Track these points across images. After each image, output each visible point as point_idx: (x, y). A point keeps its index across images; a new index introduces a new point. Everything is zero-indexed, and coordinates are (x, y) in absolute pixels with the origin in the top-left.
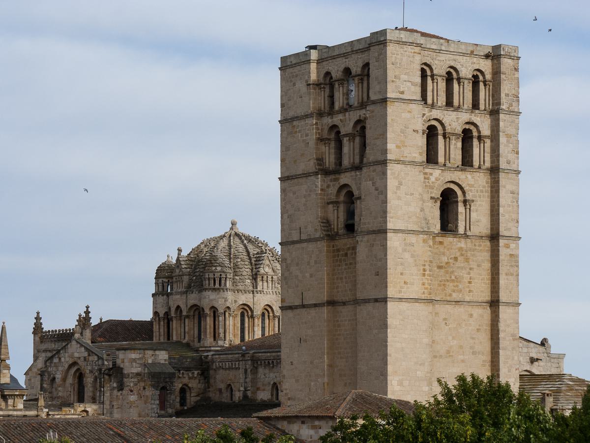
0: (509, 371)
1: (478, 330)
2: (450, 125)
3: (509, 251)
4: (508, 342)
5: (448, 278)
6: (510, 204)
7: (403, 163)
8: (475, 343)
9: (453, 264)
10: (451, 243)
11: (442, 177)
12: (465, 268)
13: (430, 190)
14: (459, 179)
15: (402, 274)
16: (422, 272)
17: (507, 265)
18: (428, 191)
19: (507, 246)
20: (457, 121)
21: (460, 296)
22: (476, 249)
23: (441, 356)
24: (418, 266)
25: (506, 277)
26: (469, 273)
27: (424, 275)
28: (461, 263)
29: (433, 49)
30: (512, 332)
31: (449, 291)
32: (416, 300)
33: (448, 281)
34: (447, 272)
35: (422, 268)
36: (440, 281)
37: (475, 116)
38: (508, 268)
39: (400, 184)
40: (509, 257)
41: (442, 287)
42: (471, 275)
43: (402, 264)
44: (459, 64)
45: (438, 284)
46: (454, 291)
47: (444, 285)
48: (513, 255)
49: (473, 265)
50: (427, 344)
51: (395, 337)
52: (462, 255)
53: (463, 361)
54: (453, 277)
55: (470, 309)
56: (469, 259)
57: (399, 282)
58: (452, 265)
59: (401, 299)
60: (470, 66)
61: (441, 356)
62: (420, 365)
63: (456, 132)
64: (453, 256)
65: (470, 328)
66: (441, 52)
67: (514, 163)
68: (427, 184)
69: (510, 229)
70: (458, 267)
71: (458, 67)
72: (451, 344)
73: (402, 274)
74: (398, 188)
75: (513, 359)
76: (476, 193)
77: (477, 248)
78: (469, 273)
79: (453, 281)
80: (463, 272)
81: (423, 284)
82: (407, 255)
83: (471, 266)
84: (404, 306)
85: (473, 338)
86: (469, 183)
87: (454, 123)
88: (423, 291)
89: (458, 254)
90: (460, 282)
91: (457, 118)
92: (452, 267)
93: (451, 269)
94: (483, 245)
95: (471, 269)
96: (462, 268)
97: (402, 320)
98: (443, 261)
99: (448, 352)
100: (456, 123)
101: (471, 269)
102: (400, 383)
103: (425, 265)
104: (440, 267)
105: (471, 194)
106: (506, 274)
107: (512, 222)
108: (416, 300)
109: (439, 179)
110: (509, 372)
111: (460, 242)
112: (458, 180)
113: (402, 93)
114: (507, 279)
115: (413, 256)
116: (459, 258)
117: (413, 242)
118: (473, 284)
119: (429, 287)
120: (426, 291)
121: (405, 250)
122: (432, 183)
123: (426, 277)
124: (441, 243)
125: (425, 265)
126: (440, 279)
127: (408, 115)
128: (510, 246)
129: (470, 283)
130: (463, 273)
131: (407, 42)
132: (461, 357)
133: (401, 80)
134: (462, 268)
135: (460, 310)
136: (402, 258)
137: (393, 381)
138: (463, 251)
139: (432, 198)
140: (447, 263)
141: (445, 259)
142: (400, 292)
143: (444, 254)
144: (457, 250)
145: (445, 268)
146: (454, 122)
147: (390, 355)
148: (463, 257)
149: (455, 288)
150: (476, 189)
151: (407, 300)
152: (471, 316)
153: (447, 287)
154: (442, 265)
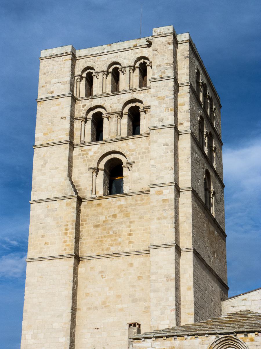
0: (162, 313)
1: (139, 278)
2: (111, 107)
3: (162, 197)
4: (161, 284)
5: (106, 234)
6: (163, 154)
7: (49, 145)
8: (135, 291)
9: (112, 221)
10: (110, 203)
11: (101, 149)
12: (125, 223)
13: (88, 163)
14: (119, 147)
15: (43, 236)
16: (64, 231)
17: (159, 210)
18: (86, 164)
19: (160, 193)
20: (118, 102)
21: (119, 249)
22: (137, 204)
23: (96, 308)
24: (60, 227)
25: (158, 222)
26: (129, 227)
27: (66, 234)
28: (120, 217)
29: (94, 54)
30: (166, 273)
31: (106, 246)
32: (55, 258)
33: (105, 237)
34: (104, 229)
35: (64, 228)
36: (97, 238)
37: (137, 93)
38: (161, 212)
39: (46, 162)
40: (161, 203)
41: (99, 243)
42: (131, 228)
43: (43, 228)
44: (121, 58)
45: (94, 241)
46: (112, 245)
47: (101, 241)
48: (166, 200)
49: (133, 217)
50: (66, 296)
51: (33, 293)
52: (121, 211)
53: (121, 310)
54: (111, 233)
55: (129, 259)
56: (129, 213)
57: (40, 244)
58: (110, 222)
59: (39, 259)
60: (132, 57)
61: (96, 308)
62: (58, 316)
63: (117, 110)
64: (112, 214)
65: (130, 277)
66: (102, 54)
67: (168, 119)
68: (86, 159)
69: (163, 177)
70: (118, 223)
71: (119, 61)
72: (108, 294)
73: (43, 236)
74: (43, 166)
75: (167, 300)
76: (138, 156)
77: (139, 202)
78: (129, 227)
79: (111, 236)
80: (123, 226)
81: (65, 242)
82: (49, 220)
83: (132, 220)
84: (43, 264)
85: (133, 286)
86: (130, 148)
87: (115, 105)
88: (64, 248)
89: (117, 211)
90: (119, 236)
91: (118, 100)
92: (111, 224)
93: (110, 226)
94: (145, 199)
95: (131, 222)
96: (121, 223)
97: (40, 277)
98: (100, 220)
99: (104, 303)
100: (118, 104)
101: (131, 222)
102: (35, 337)
103: (67, 225)
104: (97, 226)
105: (131, 157)
106: (159, 219)
107: (165, 170)
108: (55, 258)
109: (98, 152)
110: (161, 314)
111: (120, 200)
112: (119, 149)
113: (53, 92)
114: (159, 223)
115: (55, 219)
116: (118, 215)
117: (57, 207)
118: (133, 236)
119: (71, 244)
120: (67, 248)
121: (47, 216)
122: (91, 157)
123: (68, 235)
124: (99, 205)
125: (67, 225)
126: (97, 236)
127: (56, 108)
128: (162, 192)
129: (130, 235)
130: (122, 227)
131: (57, 55)
132: (119, 306)
133: (51, 84)
134: (121, 223)
135: (116, 261)
136: (44, 223)
137: (27, 335)
138: (123, 208)
139: (90, 169)
140: (104, 222)
141: (102, 218)
142: (40, 252)
143: (102, 214)
144: (116, 208)
145: (102, 225)
146: (116, 103)
147: (26, 311)
148: (122, 213)
149: (112, 242)
150: (137, 152)
151: (45, 259)
152: (131, 265)
153: (105, 242)
154: (99, 223)
